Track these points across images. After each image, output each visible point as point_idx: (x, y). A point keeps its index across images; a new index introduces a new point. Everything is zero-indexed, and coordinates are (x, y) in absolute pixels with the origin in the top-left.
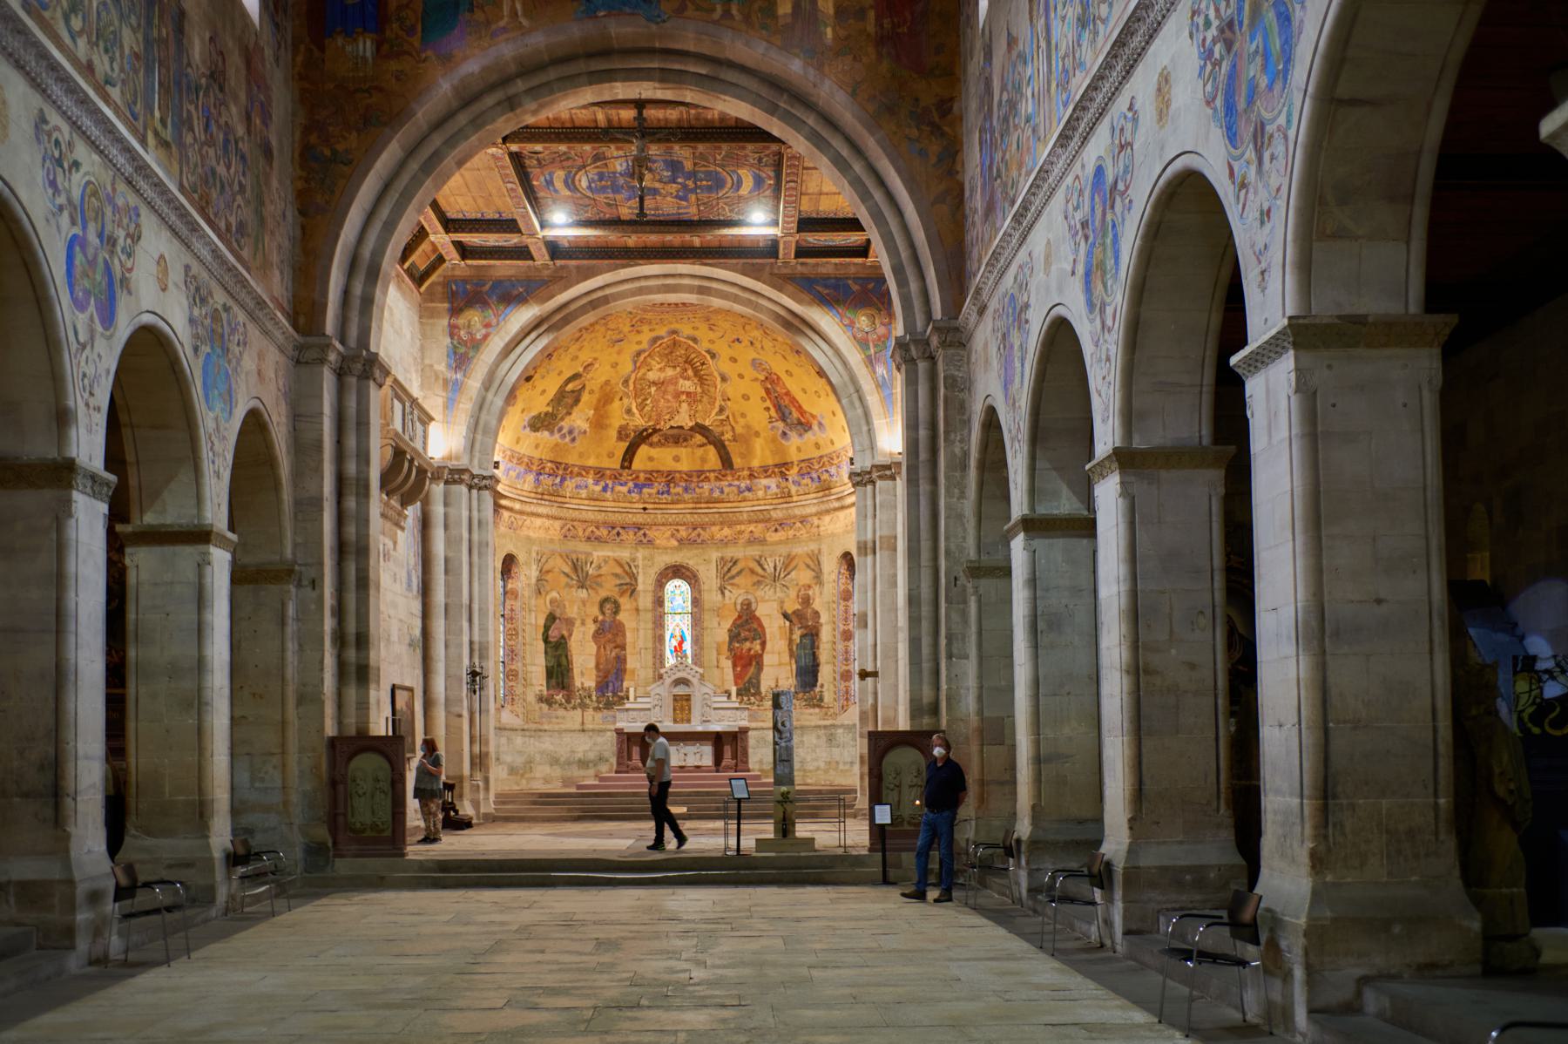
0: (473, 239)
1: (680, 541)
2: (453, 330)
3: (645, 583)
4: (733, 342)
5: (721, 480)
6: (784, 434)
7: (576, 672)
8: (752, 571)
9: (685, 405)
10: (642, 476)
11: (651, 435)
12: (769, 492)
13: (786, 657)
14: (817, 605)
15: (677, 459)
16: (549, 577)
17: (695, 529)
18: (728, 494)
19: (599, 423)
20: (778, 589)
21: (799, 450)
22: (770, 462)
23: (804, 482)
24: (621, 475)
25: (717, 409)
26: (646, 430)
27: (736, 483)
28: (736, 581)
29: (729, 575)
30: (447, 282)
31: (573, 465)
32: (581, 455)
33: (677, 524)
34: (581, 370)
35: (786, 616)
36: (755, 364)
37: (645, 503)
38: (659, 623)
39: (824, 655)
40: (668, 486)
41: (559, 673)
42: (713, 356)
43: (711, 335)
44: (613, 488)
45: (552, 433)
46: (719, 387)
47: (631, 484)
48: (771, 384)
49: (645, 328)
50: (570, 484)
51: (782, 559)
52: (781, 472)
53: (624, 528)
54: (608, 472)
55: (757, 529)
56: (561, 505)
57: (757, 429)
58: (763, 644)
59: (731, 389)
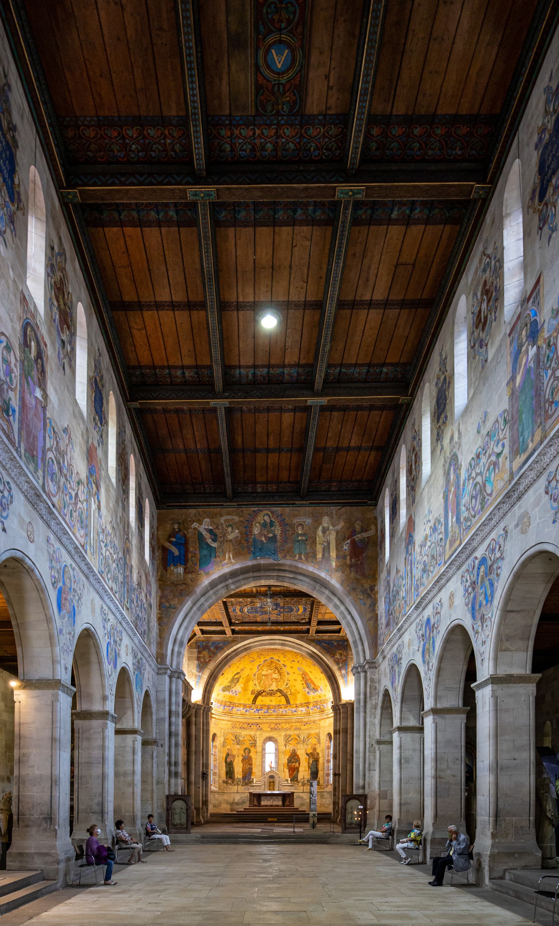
0: (205, 628)
1: (272, 729)
2: (198, 659)
3: (259, 743)
7: (236, 773)
9: (274, 683)
13: (307, 768)
14: (318, 751)
15: (271, 701)
16: (227, 741)
19: (245, 689)
30: (197, 642)
32: (239, 700)
35: (307, 754)
36: (299, 669)
38: (263, 756)
39: (320, 768)
41: (230, 773)
42: (285, 666)
48: (304, 676)
50: (235, 709)
55: (298, 725)
56: (232, 717)
58: (299, 764)
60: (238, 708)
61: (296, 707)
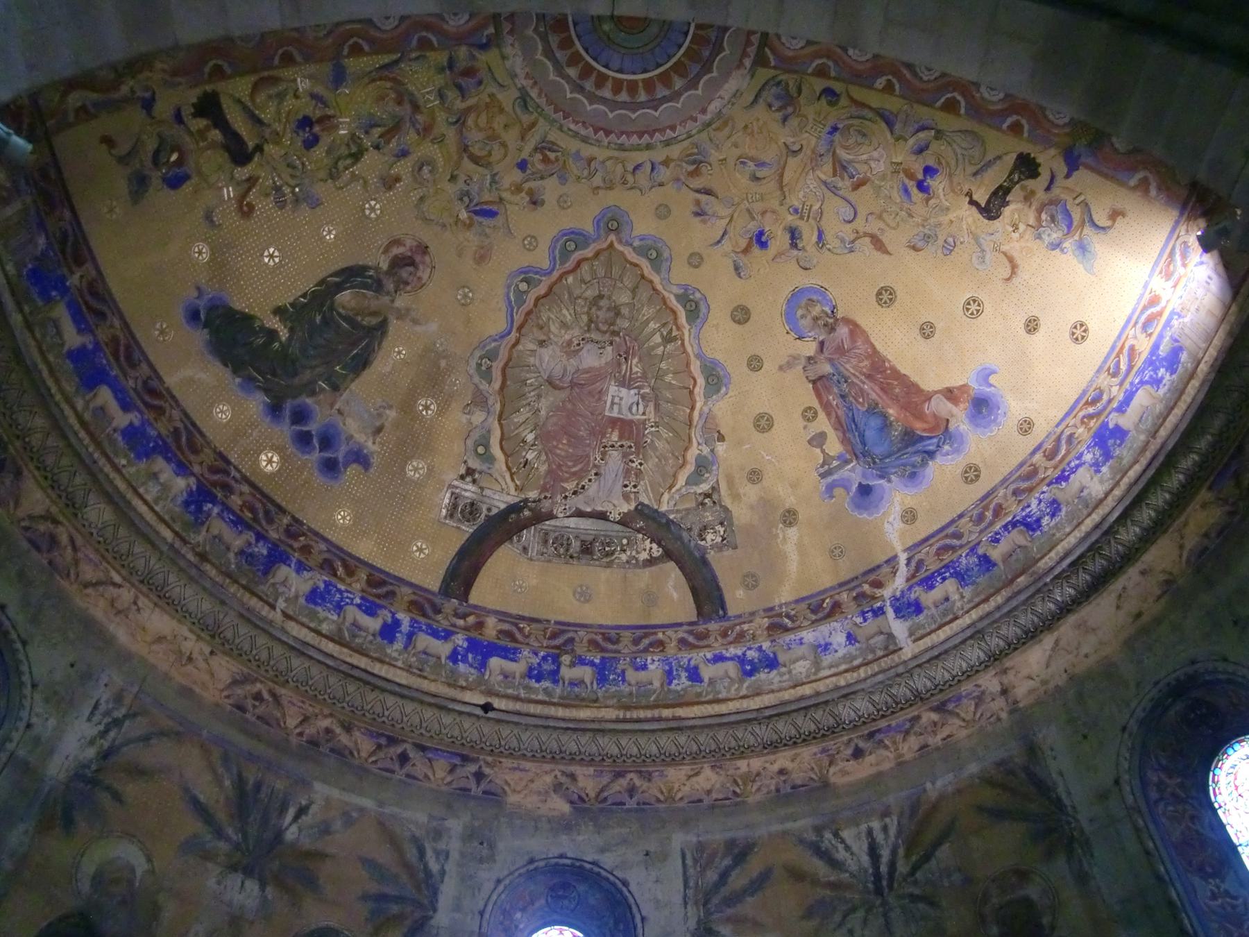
1: (579, 803)
4: (746, 251)
5: (693, 647)
6: (865, 490)
8: (797, 875)
10: (492, 627)
11: (526, 525)
12: (827, 659)
17: (619, 775)
18: (712, 682)
20: (895, 915)
21: (909, 516)
22: (827, 581)
23: (937, 593)
24: (438, 611)
25: (690, 468)
26: (514, 509)
27: (734, 651)
28: (749, 907)
29: (725, 891)
31: (316, 534)
33: (572, 760)
34: (384, 266)
37: (490, 693)
40: (556, 659)
43: (699, 235)
44: (410, 636)
45: (275, 410)
46: (698, 405)
47: (460, 640)
49: (550, 189)
51: (892, 823)
52: (861, 597)
53: (422, 748)
54: (406, 590)
57: (790, 501)
59: (722, 408)
60: (320, 579)
61: (776, 628)
